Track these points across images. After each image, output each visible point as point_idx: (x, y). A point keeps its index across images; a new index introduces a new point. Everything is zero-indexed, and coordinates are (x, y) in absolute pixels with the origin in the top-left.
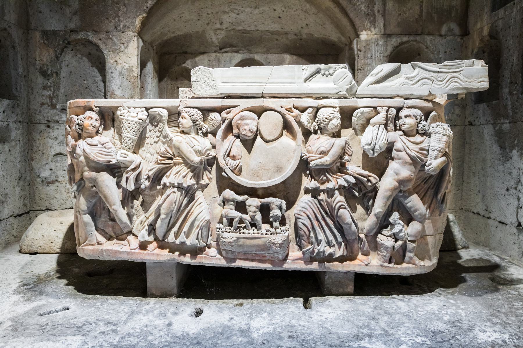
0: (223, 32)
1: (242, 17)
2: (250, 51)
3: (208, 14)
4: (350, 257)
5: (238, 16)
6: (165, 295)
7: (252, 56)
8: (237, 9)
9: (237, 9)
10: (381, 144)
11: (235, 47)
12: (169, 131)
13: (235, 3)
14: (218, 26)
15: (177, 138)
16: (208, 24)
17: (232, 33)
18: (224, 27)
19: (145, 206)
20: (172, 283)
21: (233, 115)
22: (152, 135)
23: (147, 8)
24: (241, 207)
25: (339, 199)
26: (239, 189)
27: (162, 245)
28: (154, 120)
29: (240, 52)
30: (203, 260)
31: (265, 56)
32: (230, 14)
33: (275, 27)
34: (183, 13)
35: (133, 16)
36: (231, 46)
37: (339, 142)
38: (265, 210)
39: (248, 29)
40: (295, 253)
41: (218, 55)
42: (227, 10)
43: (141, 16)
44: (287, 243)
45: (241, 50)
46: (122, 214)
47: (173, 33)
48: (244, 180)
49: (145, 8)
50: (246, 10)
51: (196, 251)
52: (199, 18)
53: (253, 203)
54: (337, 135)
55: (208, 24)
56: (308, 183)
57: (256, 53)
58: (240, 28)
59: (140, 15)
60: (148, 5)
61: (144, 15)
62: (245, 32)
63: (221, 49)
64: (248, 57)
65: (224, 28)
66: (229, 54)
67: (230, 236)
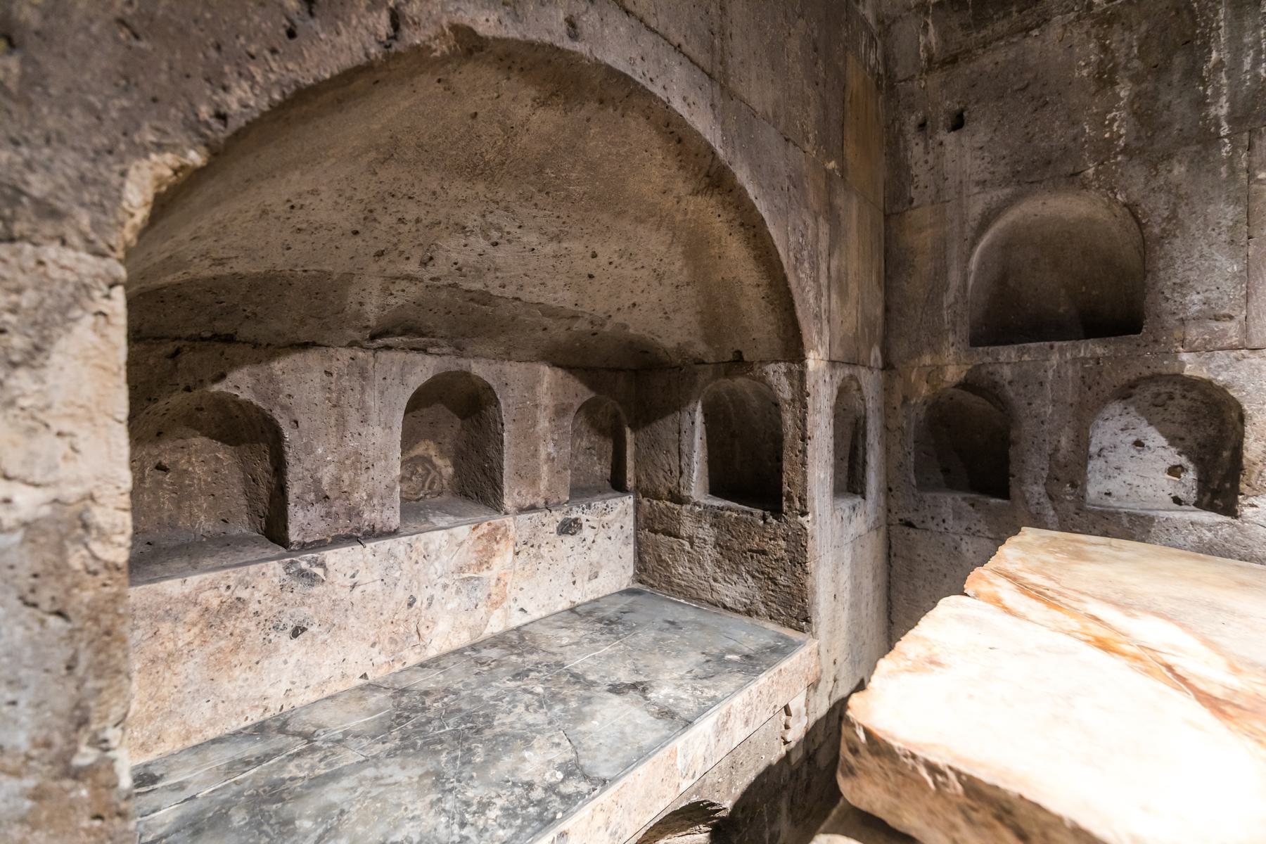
0: (413, 289)
1: (501, 255)
2: (459, 351)
3: (401, 220)
5: (490, 250)
7: (463, 364)
8: (499, 229)
9: (499, 229)
11: (423, 335)
13: (506, 209)
14: (412, 267)
16: (380, 254)
17: (444, 295)
18: (432, 271)
23: (222, 117)
29: (430, 350)
31: (498, 366)
32: (472, 239)
33: (563, 298)
34: (314, 192)
35: (100, 140)
36: (408, 330)
39: (496, 292)
41: (361, 354)
42: (470, 224)
43: (169, 158)
45: (433, 345)
47: (220, 262)
49: (205, 111)
50: (525, 239)
52: (358, 228)
55: (380, 254)
57: (475, 356)
58: (478, 286)
59: (160, 148)
60: (232, 103)
61: (195, 158)
62: (485, 298)
63: (373, 338)
64: (454, 368)
65: (427, 277)
66: (398, 356)
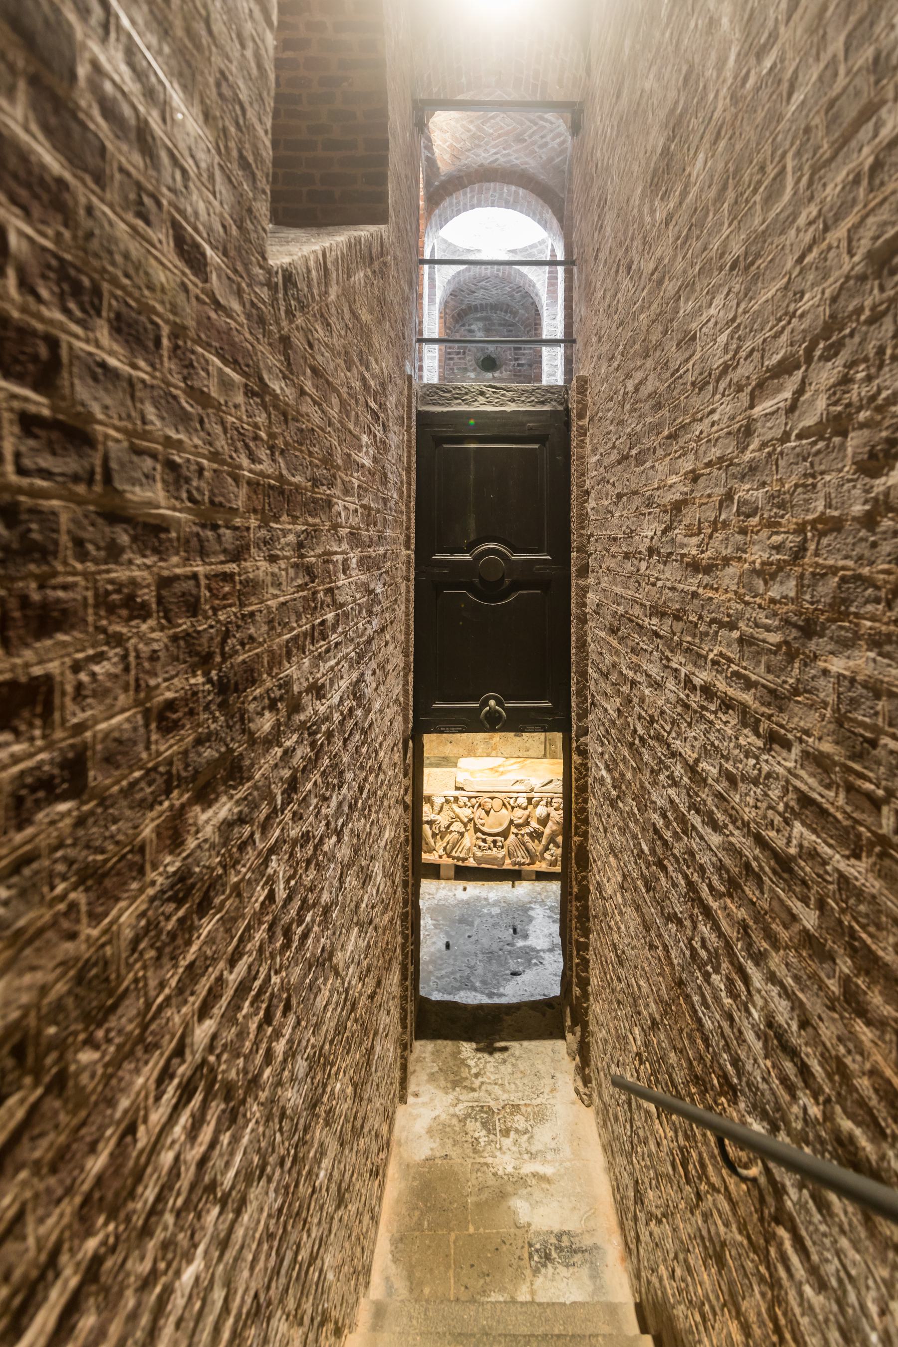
4: (533, 863)
6: (448, 879)
10: (544, 814)
12: (454, 806)
15: (457, 810)
19: (442, 838)
20: (452, 873)
21: (482, 800)
22: (446, 807)
24: (484, 841)
25: (526, 838)
26: (484, 833)
27: (449, 856)
28: (447, 801)
30: (467, 864)
37: (526, 812)
38: (495, 842)
40: (508, 861)
44: (504, 858)
46: (432, 841)
48: (485, 829)
51: (464, 860)
53: (489, 839)
54: (525, 809)
56: (513, 830)
67: (479, 854)
